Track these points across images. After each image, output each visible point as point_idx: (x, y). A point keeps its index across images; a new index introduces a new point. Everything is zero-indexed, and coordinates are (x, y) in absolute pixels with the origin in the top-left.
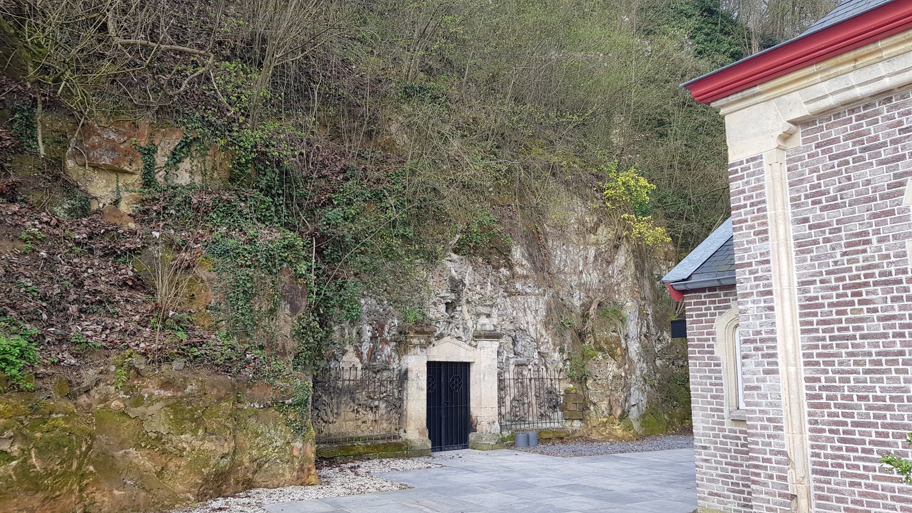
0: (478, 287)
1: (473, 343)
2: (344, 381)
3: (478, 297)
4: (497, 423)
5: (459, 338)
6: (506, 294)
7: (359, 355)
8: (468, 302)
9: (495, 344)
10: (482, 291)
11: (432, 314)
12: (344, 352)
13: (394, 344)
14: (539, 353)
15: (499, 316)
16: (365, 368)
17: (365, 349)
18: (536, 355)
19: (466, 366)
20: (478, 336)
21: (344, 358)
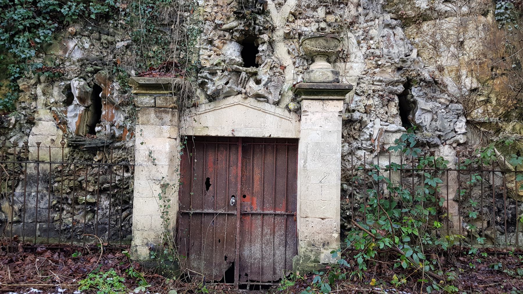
0: (321, 12)
1: (292, 106)
2: (38, 162)
3: (314, 27)
4: (335, 245)
5: (257, 96)
6: (394, 22)
7: (62, 124)
8: (287, 37)
9: (335, 108)
10: (331, 18)
11: (206, 57)
12: (31, 122)
13: (129, 108)
14: (468, 122)
15: (366, 57)
16: (75, 146)
17: (74, 115)
18: (461, 125)
19: (290, 145)
20: (301, 92)
21: (34, 130)
